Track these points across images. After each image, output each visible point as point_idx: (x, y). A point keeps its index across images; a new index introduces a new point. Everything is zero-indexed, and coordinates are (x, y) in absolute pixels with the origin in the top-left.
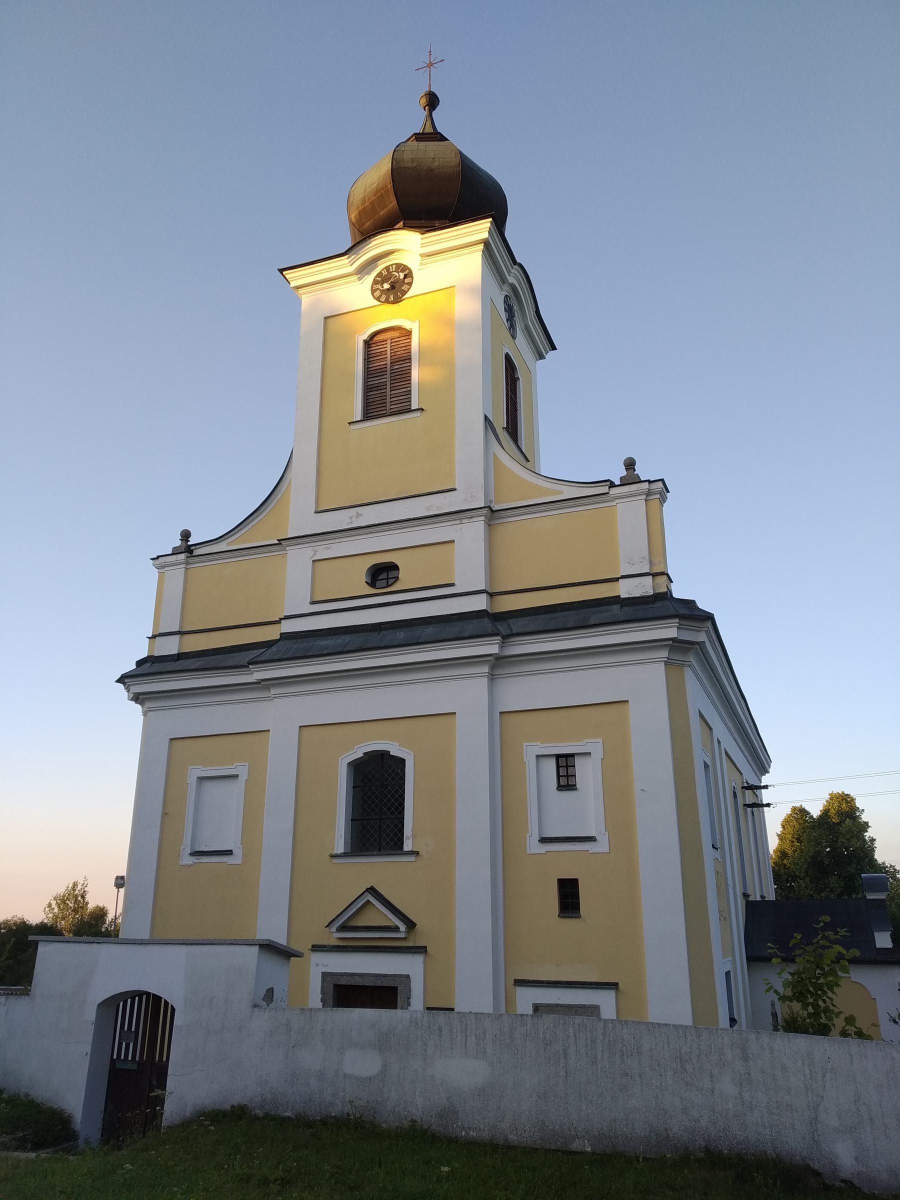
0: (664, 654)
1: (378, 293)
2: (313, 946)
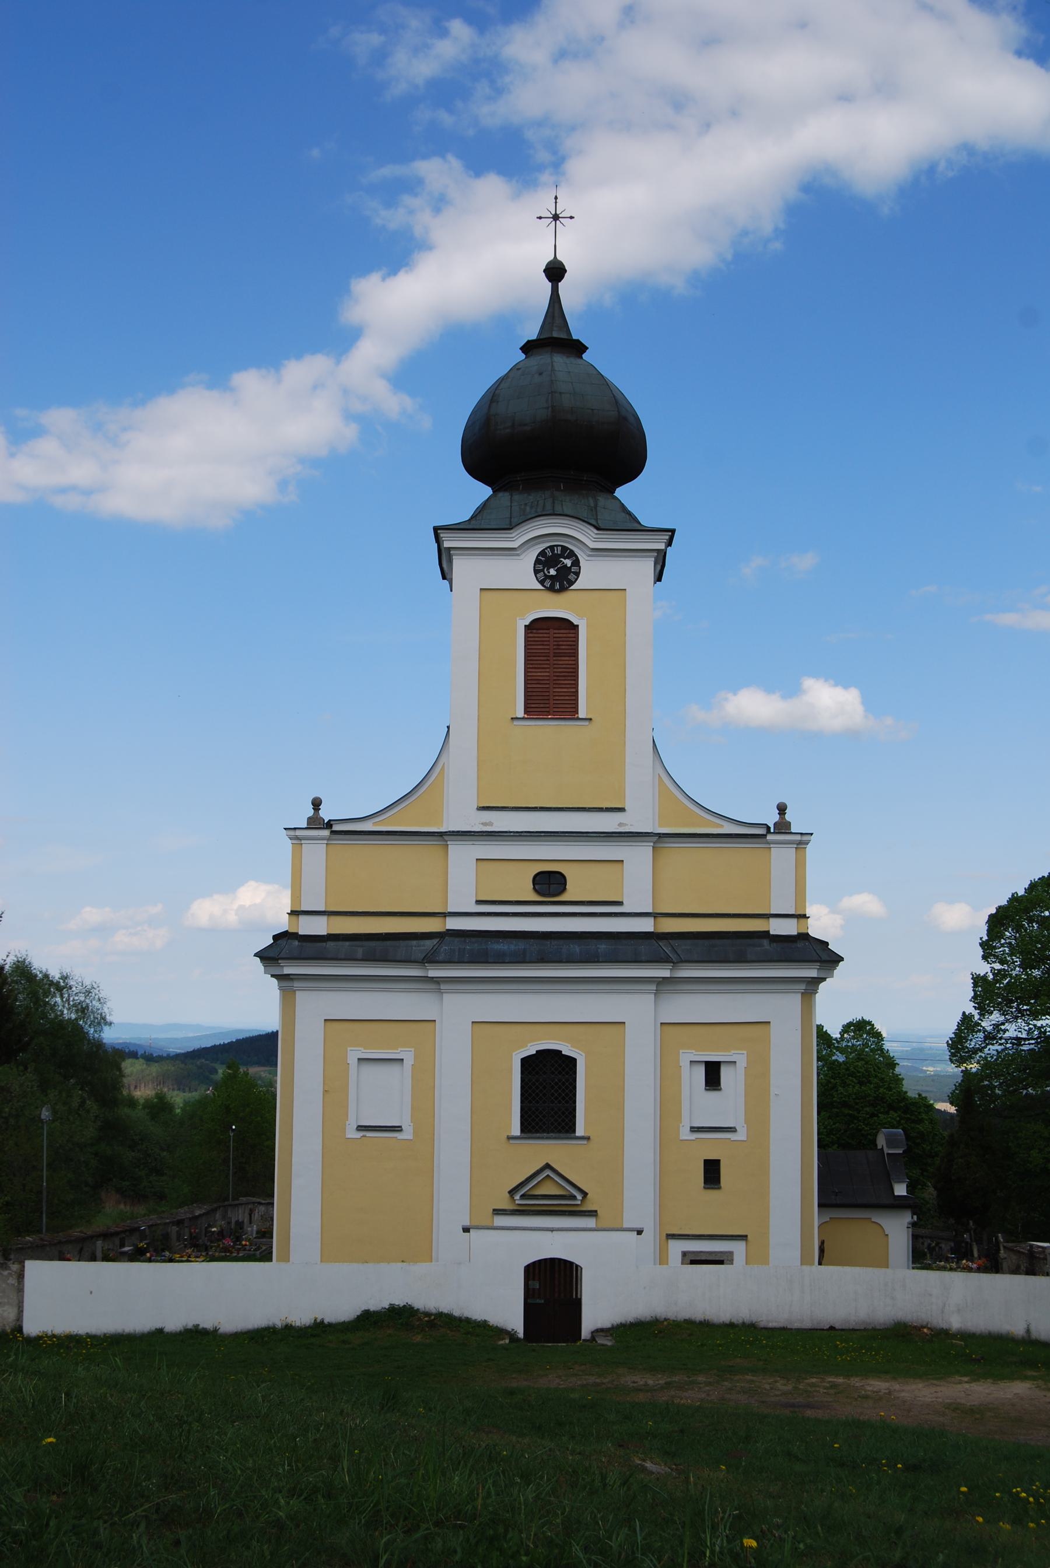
0: (803, 987)
1: (541, 575)
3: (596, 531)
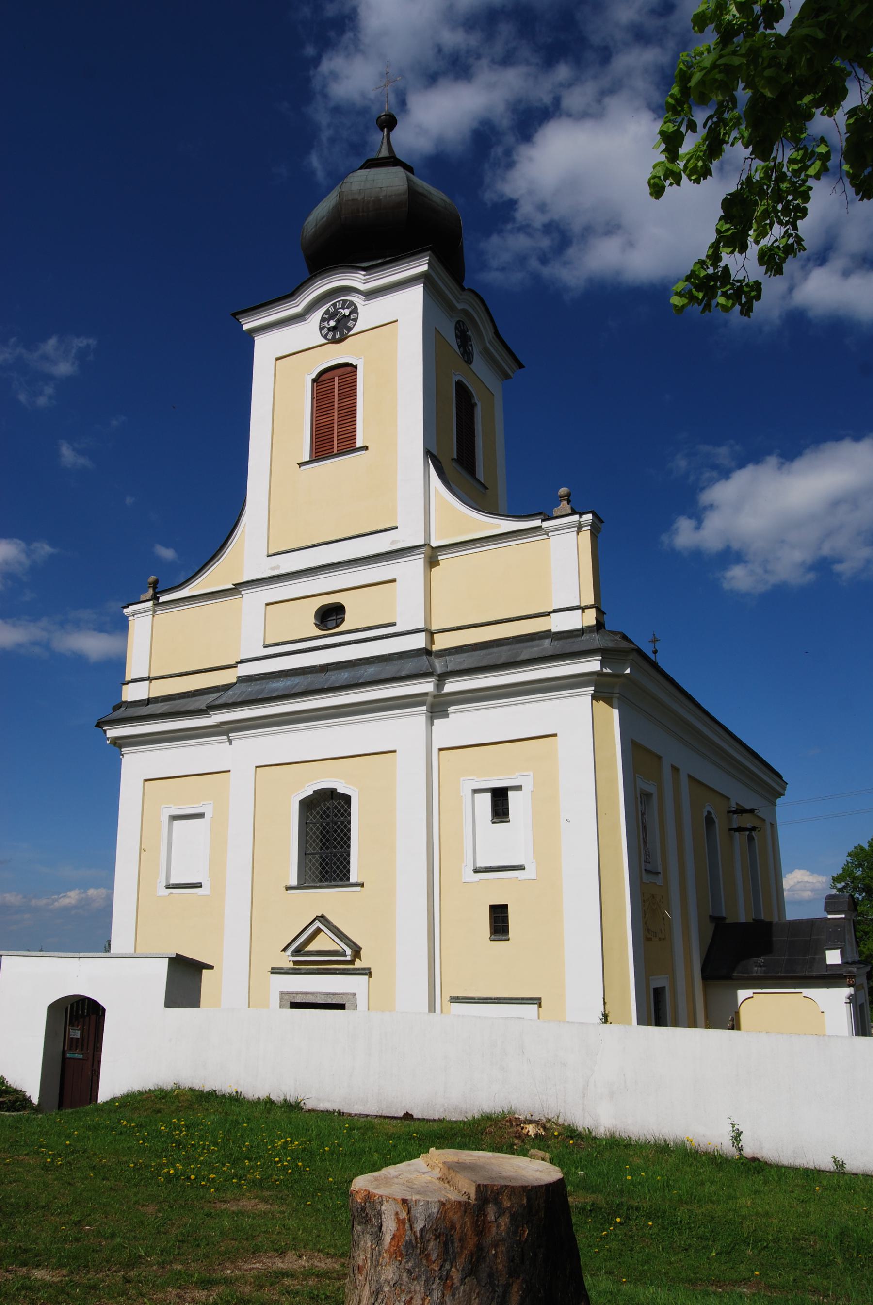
1: (325, 331)
2: (272, 968)
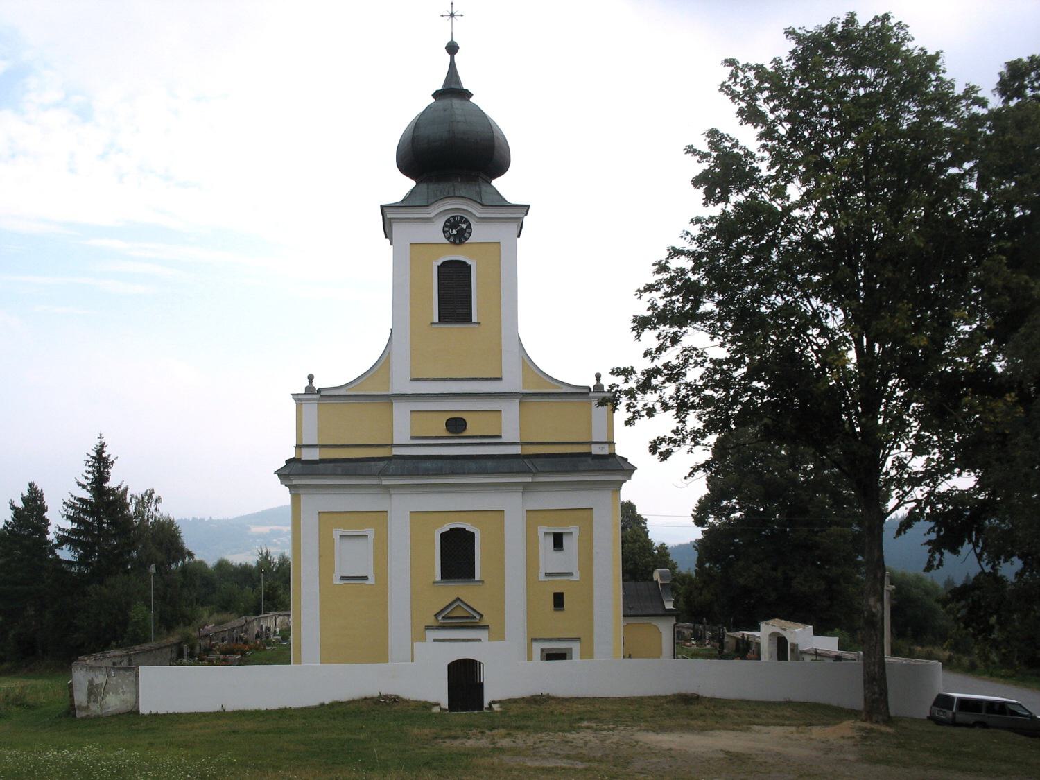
1: (447, 234)
3: (481, 207)
